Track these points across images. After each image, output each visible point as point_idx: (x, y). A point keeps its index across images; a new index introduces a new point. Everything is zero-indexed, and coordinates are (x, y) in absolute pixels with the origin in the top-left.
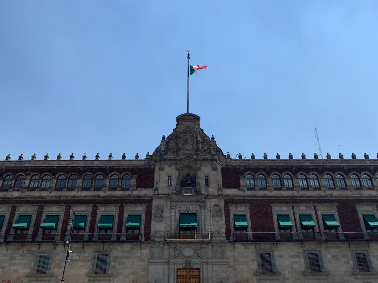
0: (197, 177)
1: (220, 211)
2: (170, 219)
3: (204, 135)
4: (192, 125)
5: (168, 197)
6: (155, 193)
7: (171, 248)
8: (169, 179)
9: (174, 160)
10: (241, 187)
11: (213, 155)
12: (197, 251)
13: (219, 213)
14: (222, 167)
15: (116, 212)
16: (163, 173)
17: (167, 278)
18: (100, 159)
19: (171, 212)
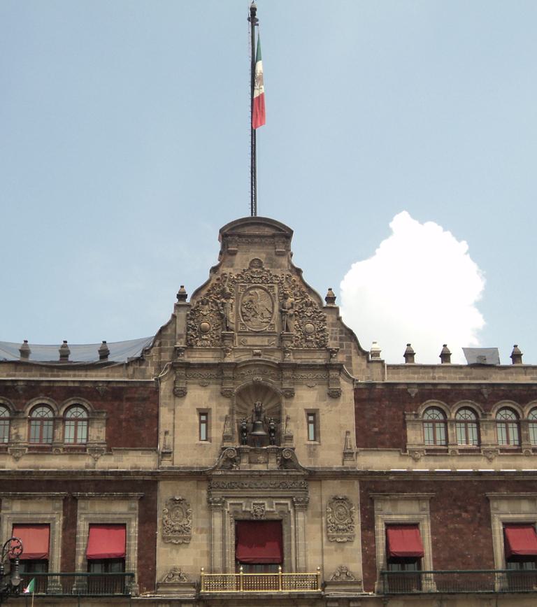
0: (284, 417)
3: (304, 289)
5: (199, 476)
8: (206, 422)
9: (214, 365)
11: (331, 352)
15: (54, 516)
19: (211, 517)
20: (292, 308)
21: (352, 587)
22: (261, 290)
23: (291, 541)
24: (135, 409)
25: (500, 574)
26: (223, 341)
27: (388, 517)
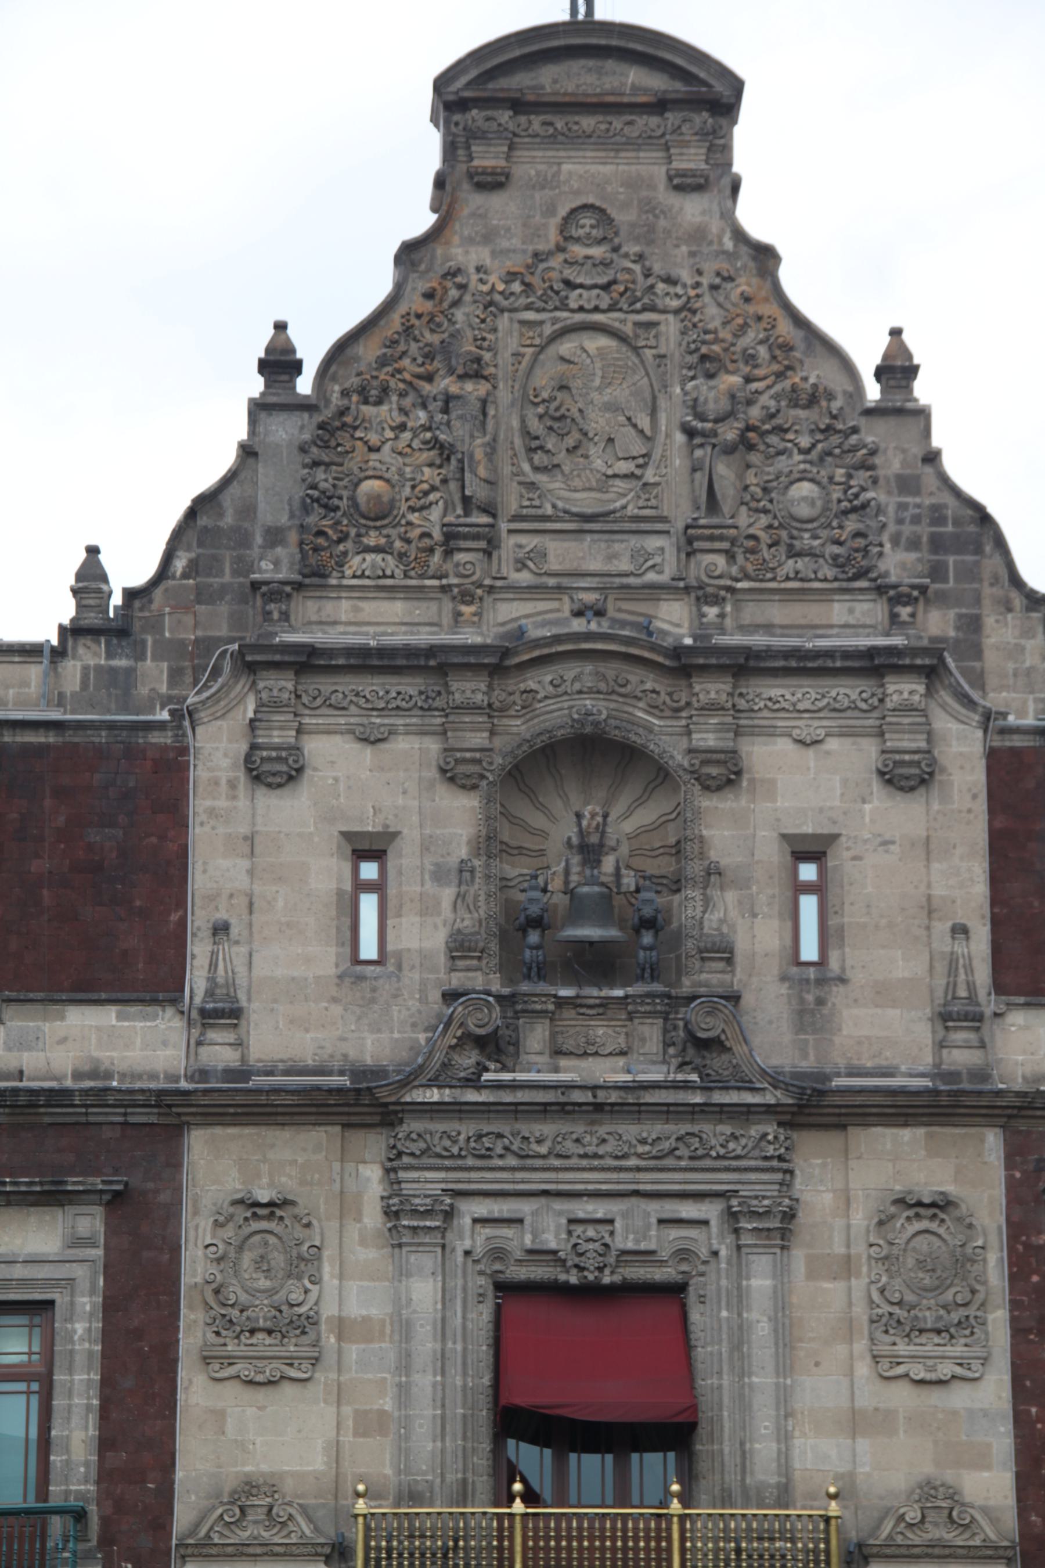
1: (965, 1262)
2: (387, 1349)
3: (785, 328)
4: (632, 184)
5: (357, 1104)
6: (203, 1050)
8: (378, 887)
13: (939, 1288)
14: (997, 742)
16: (288, 812)
22: (603, 341)
24: (94, 836)
26: (448, 553)
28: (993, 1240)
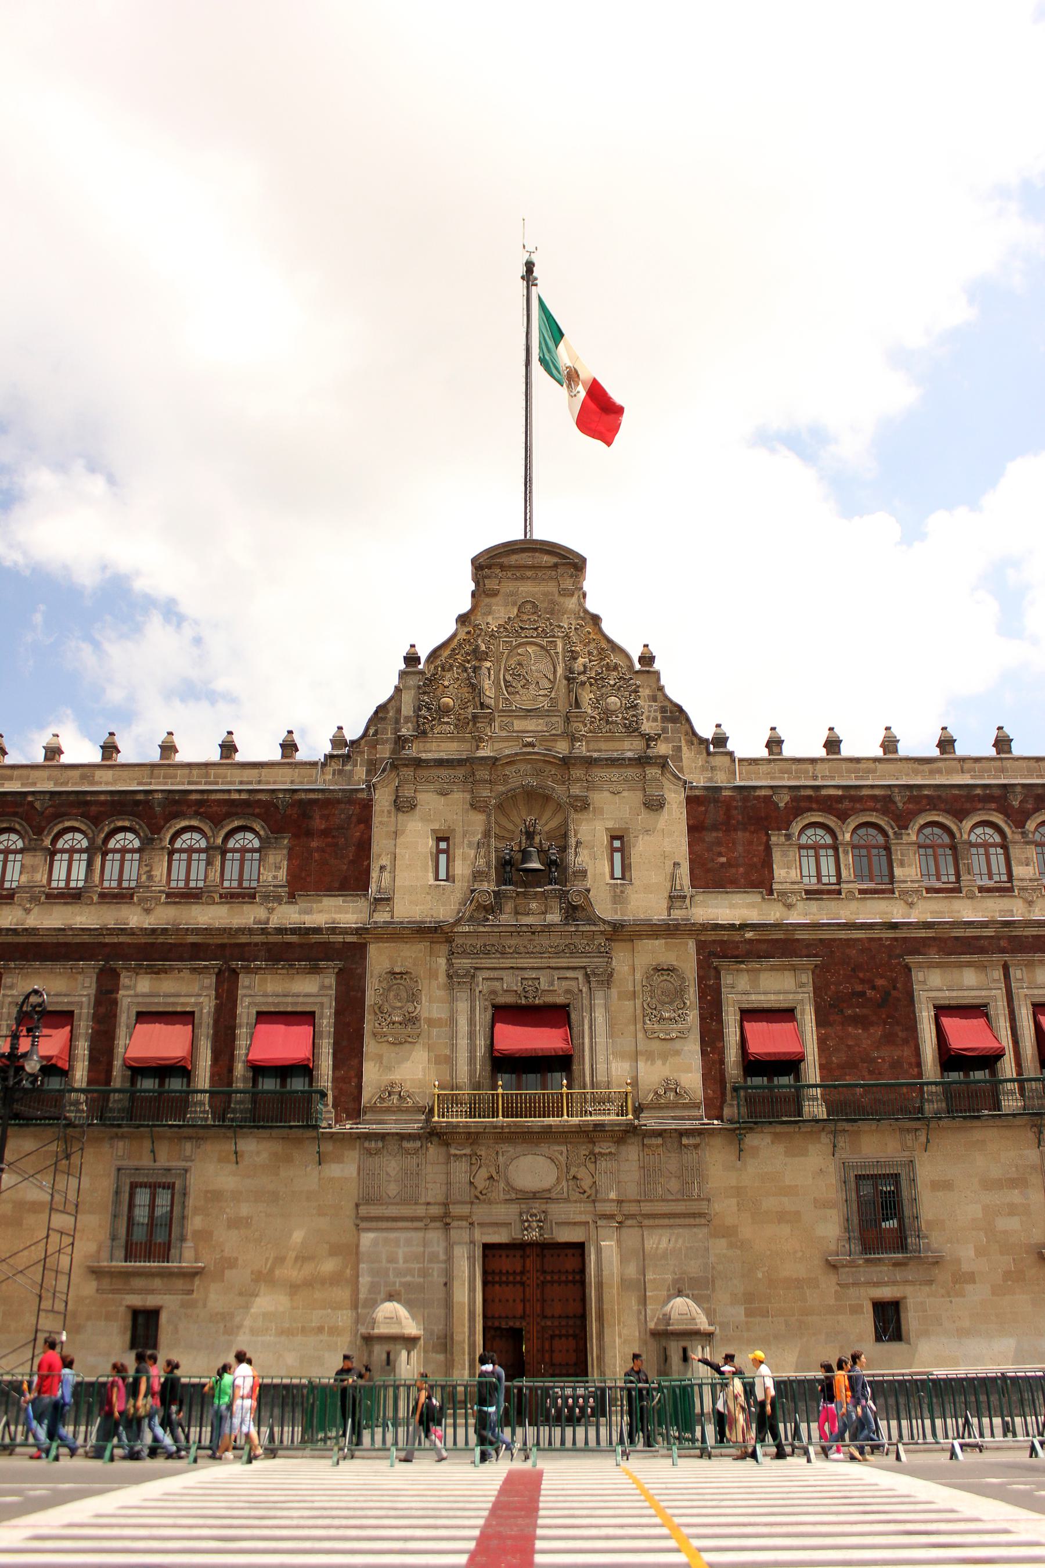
0: (572, 841)
4: (545, 594)
7: (455, 1155)
8: (446, 851)
9: (460, 762)
10: (775, 886)
11: (649, 739)
12: (573, 1171)
14: (689, 793)
15: (201, 999)
17: (443, 1280)
18: (121, 758)
19: (453, 1000)
20: (584, 672)
21: (686, 1113)
22: (535, 648)
23: (583, 1038)
25: (933, 1088)
26: (475, 724)
27: (745, 997)
28: (692, 983)
